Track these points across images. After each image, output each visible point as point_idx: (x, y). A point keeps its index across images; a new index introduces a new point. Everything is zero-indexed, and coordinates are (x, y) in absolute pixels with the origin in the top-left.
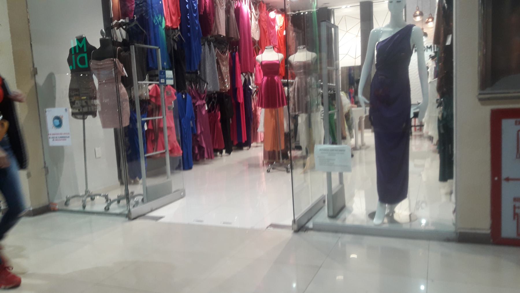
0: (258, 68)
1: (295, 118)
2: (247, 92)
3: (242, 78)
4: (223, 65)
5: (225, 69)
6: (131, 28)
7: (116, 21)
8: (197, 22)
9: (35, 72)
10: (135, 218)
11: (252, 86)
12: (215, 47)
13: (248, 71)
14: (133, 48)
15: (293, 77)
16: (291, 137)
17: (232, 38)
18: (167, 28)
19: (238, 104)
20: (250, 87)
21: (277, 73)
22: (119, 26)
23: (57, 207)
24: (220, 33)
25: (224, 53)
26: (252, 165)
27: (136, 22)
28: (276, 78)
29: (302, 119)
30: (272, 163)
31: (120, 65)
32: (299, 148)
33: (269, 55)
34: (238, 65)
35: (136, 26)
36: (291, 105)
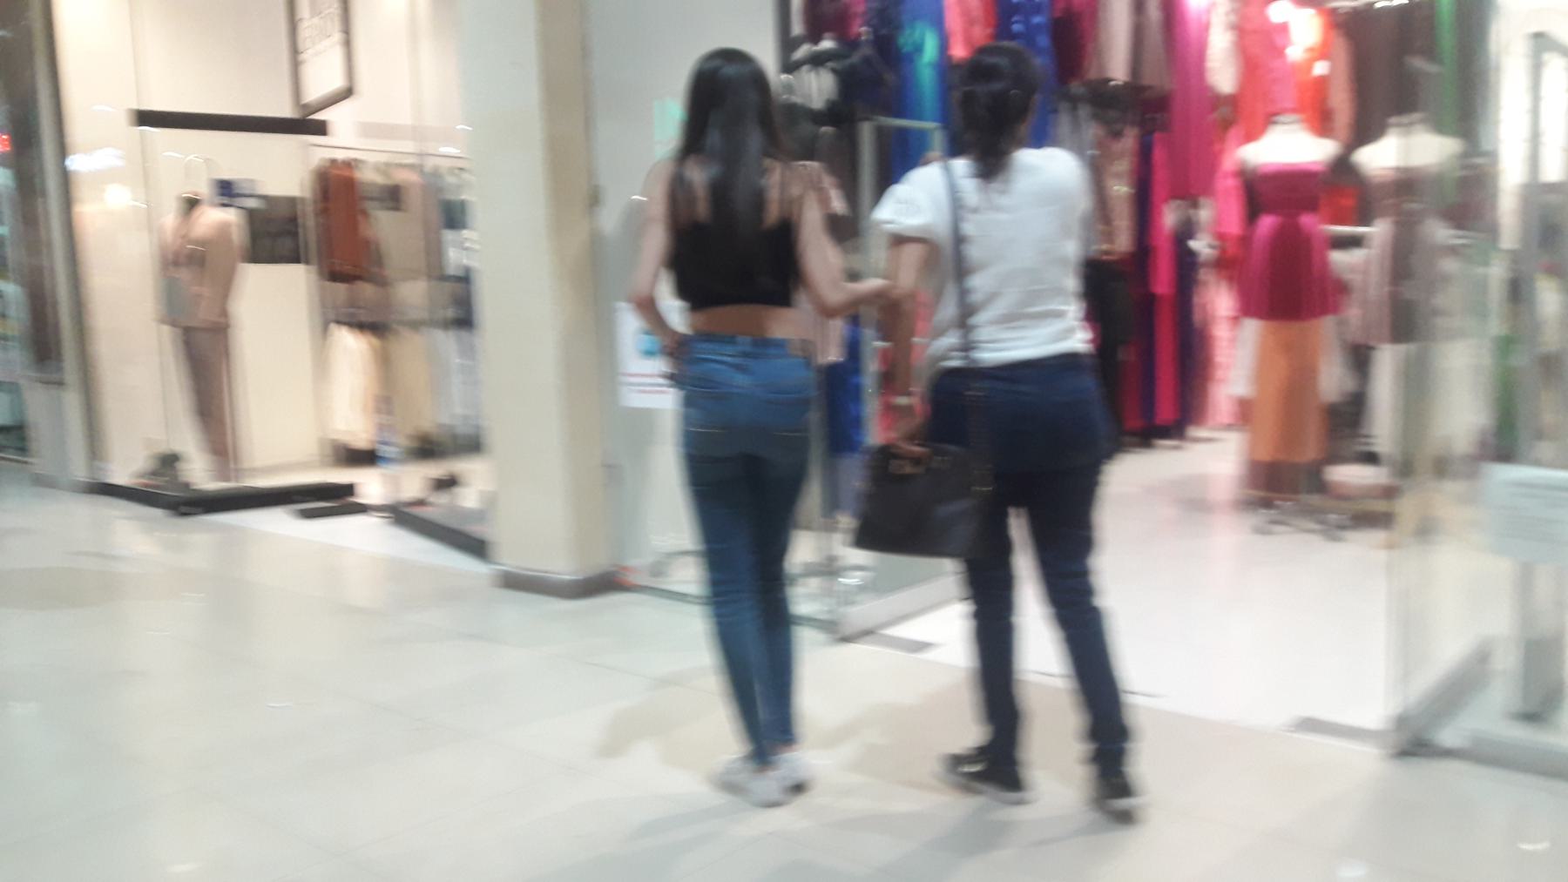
0: (1227, 185)
1: (1360, 358)
2: (1186, 263)
3: (1169, 217)
4: (1118, 176)
5: (1121, 189)
6: (853, 67)
7: (803, 51)
8: (1044, 41)
9: (594, 200)
10: (846, 639)
11: (1201, 245)
12: (1095, 117)
13: (1188, 194)
14: (866, 133)
15: (1365, 220)
16: (1345, 422)
17: (1150, 87)
18: (946, 66)
19: (1148, 303)
20: (1194, 244)
21: (1311, 206)
22: (817, 61)
23: (634, 579)
24: (1111, 74)
25: (1117, 135)
26: (1192, 503)
27: (867, 51)
28: (1307, 220)
29: (1387, 361)
30: (1267, 504)
31: (828, 181)
32: (1371, 458)
33: (1289, 146)
34: (1161, 176)
35: (867, 60)
36: (1353, 313)
